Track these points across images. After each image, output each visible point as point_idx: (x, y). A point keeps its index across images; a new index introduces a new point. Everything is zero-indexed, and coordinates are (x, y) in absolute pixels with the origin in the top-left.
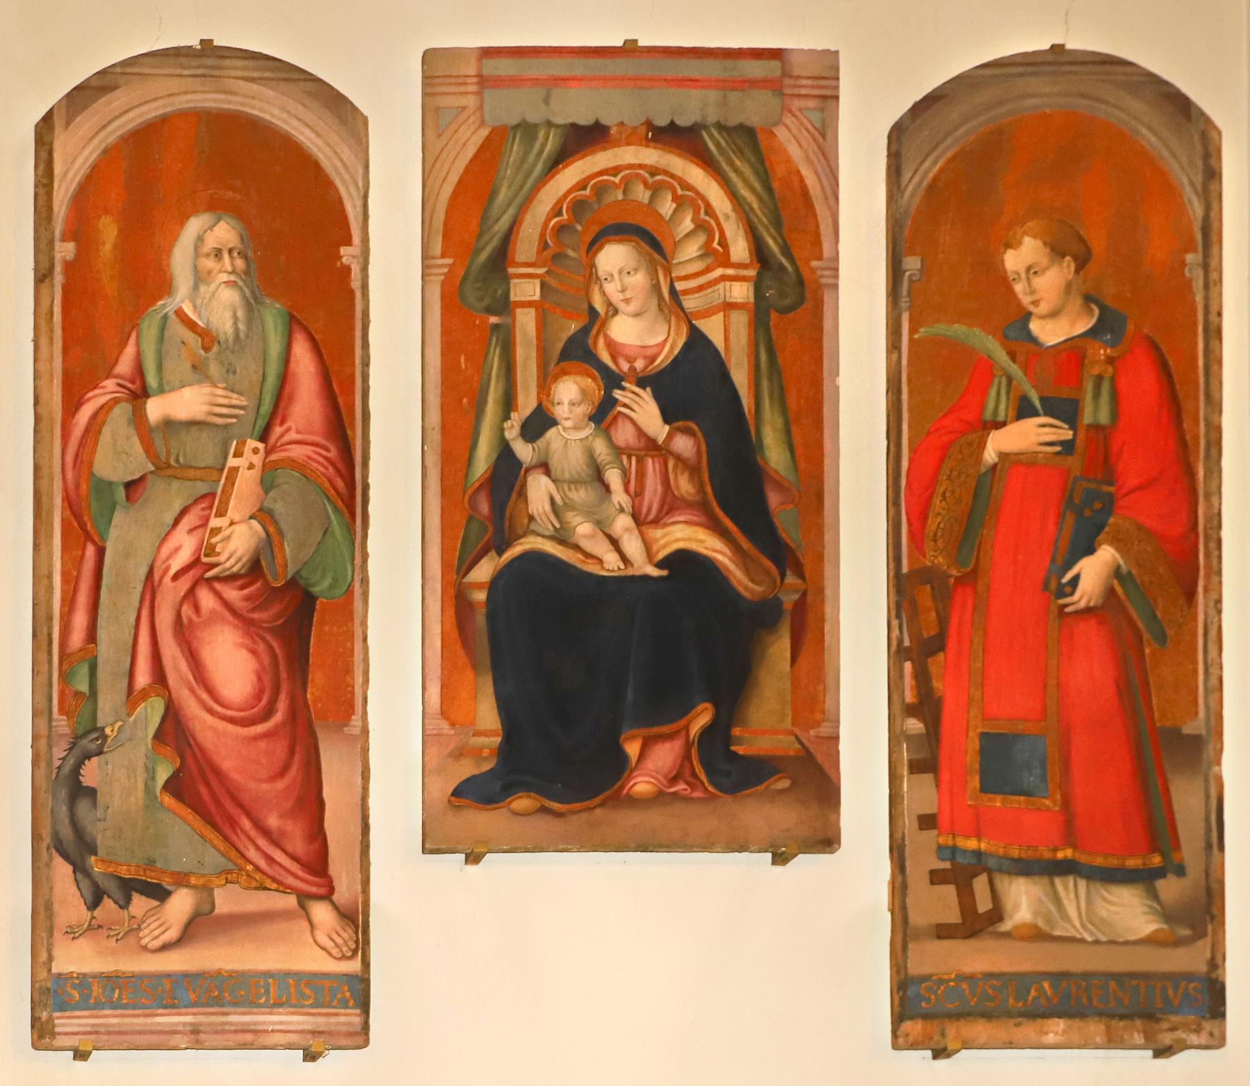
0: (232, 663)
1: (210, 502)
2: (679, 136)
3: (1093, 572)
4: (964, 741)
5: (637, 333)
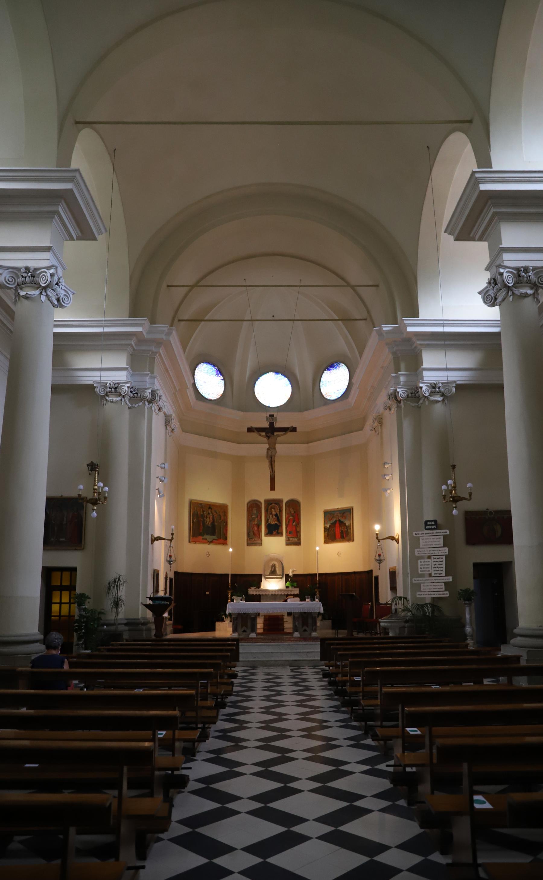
0: (256, 528)
1: (255, 521)
2: (276, 504)
3: (294, 524)
4: (289, 531)
5: (274, 513)
